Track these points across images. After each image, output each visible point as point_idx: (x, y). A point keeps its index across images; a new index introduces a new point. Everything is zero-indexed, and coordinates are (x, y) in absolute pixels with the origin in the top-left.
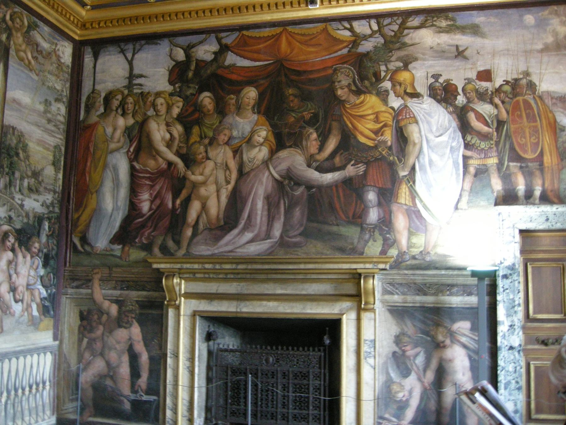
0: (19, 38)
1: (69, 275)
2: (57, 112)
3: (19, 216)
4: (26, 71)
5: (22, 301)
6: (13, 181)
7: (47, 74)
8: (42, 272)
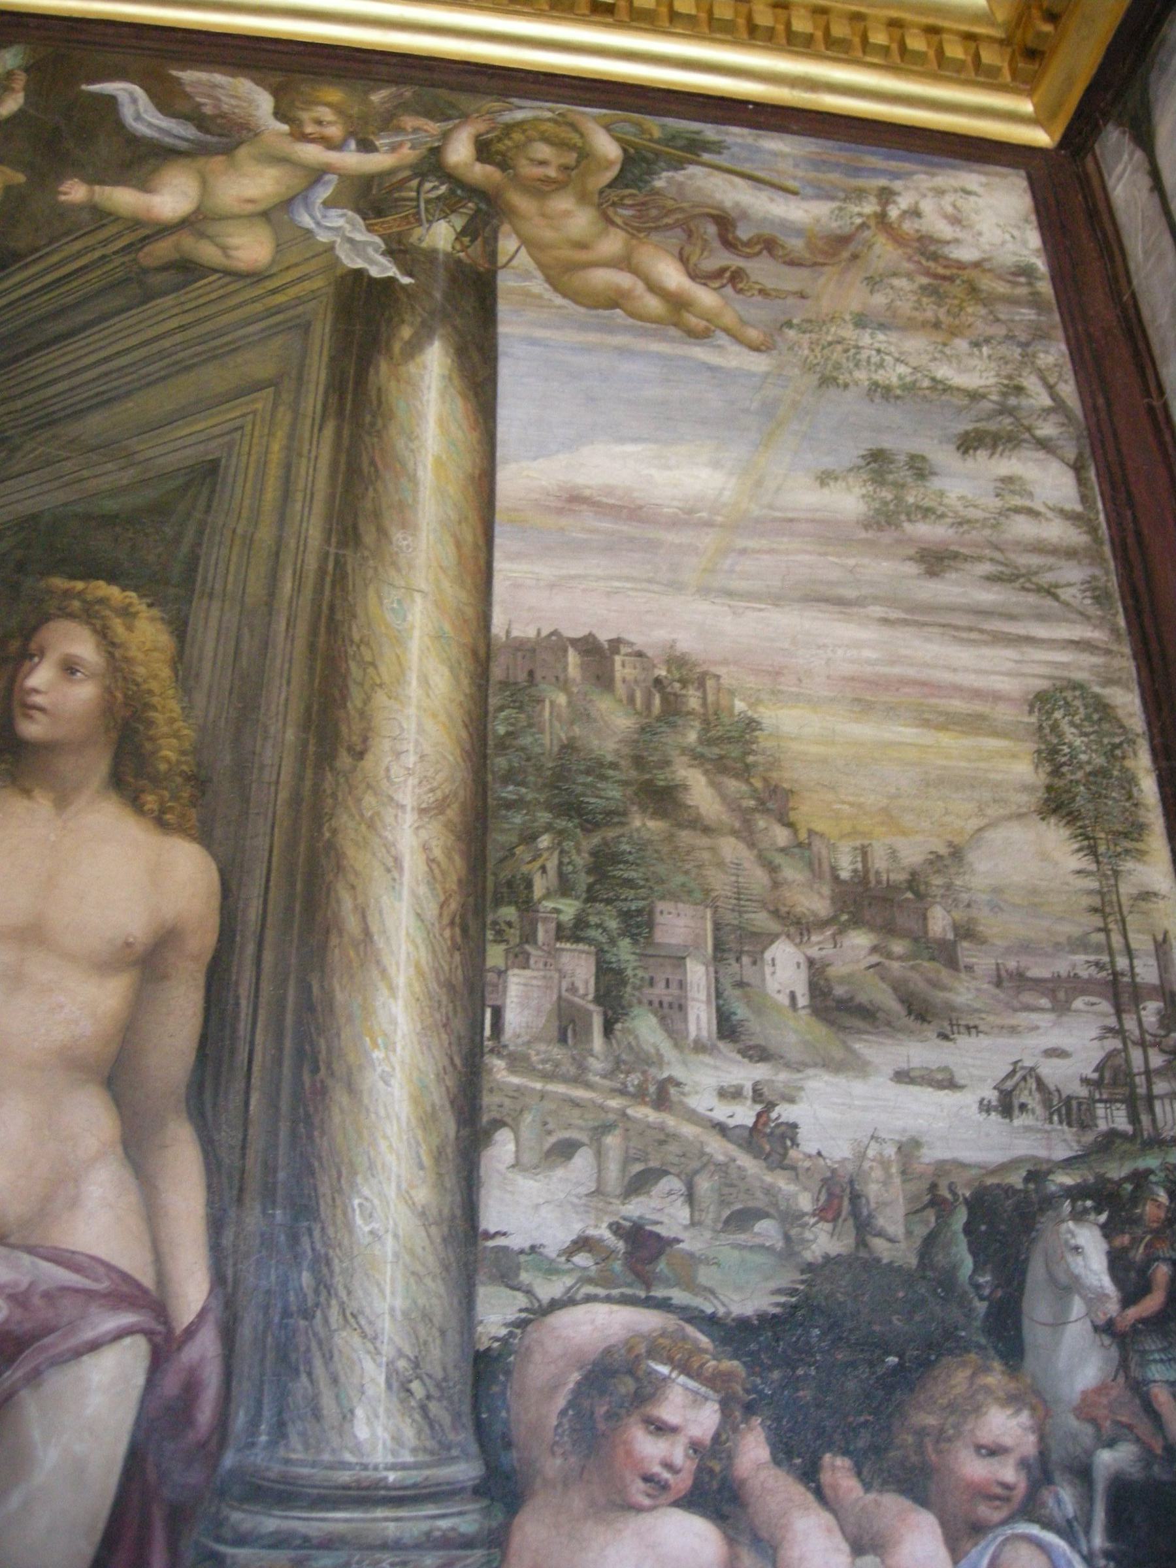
2: (996, 503)
3: (742, 1219)
7: (849, 332)
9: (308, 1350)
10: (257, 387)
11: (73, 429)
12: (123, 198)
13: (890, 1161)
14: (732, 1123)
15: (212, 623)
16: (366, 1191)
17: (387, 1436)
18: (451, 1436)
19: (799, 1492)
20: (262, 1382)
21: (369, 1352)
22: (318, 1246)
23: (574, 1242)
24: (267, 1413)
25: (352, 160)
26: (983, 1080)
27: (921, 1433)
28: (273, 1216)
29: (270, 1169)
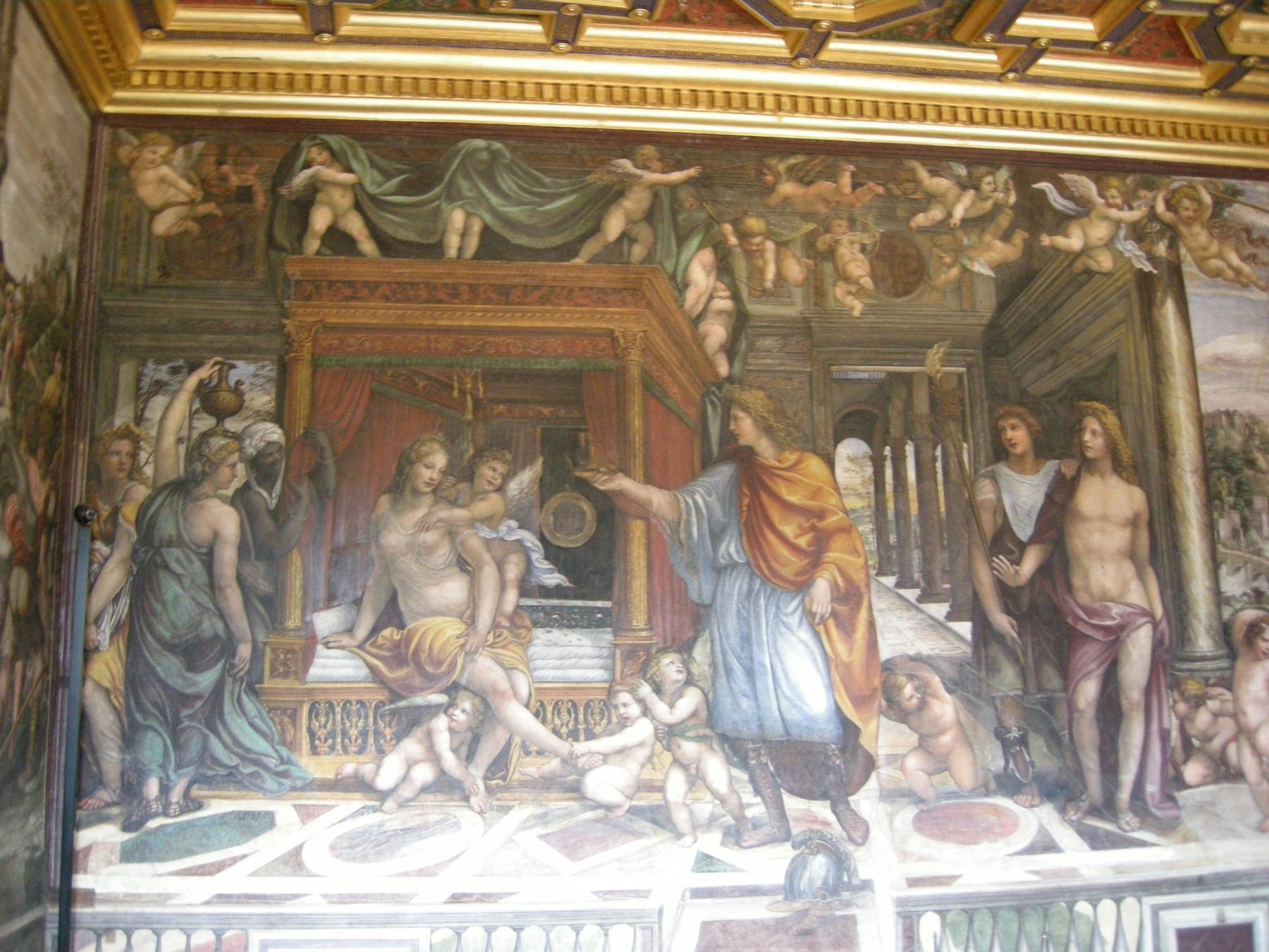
0: (1198, 235)
4: (1234, 293)
6: (1249, 518)
10: (1119, 324)
11: (1072, 344)
12: (1060, 241)
15: (1128, 413)
25: (1128, 215)
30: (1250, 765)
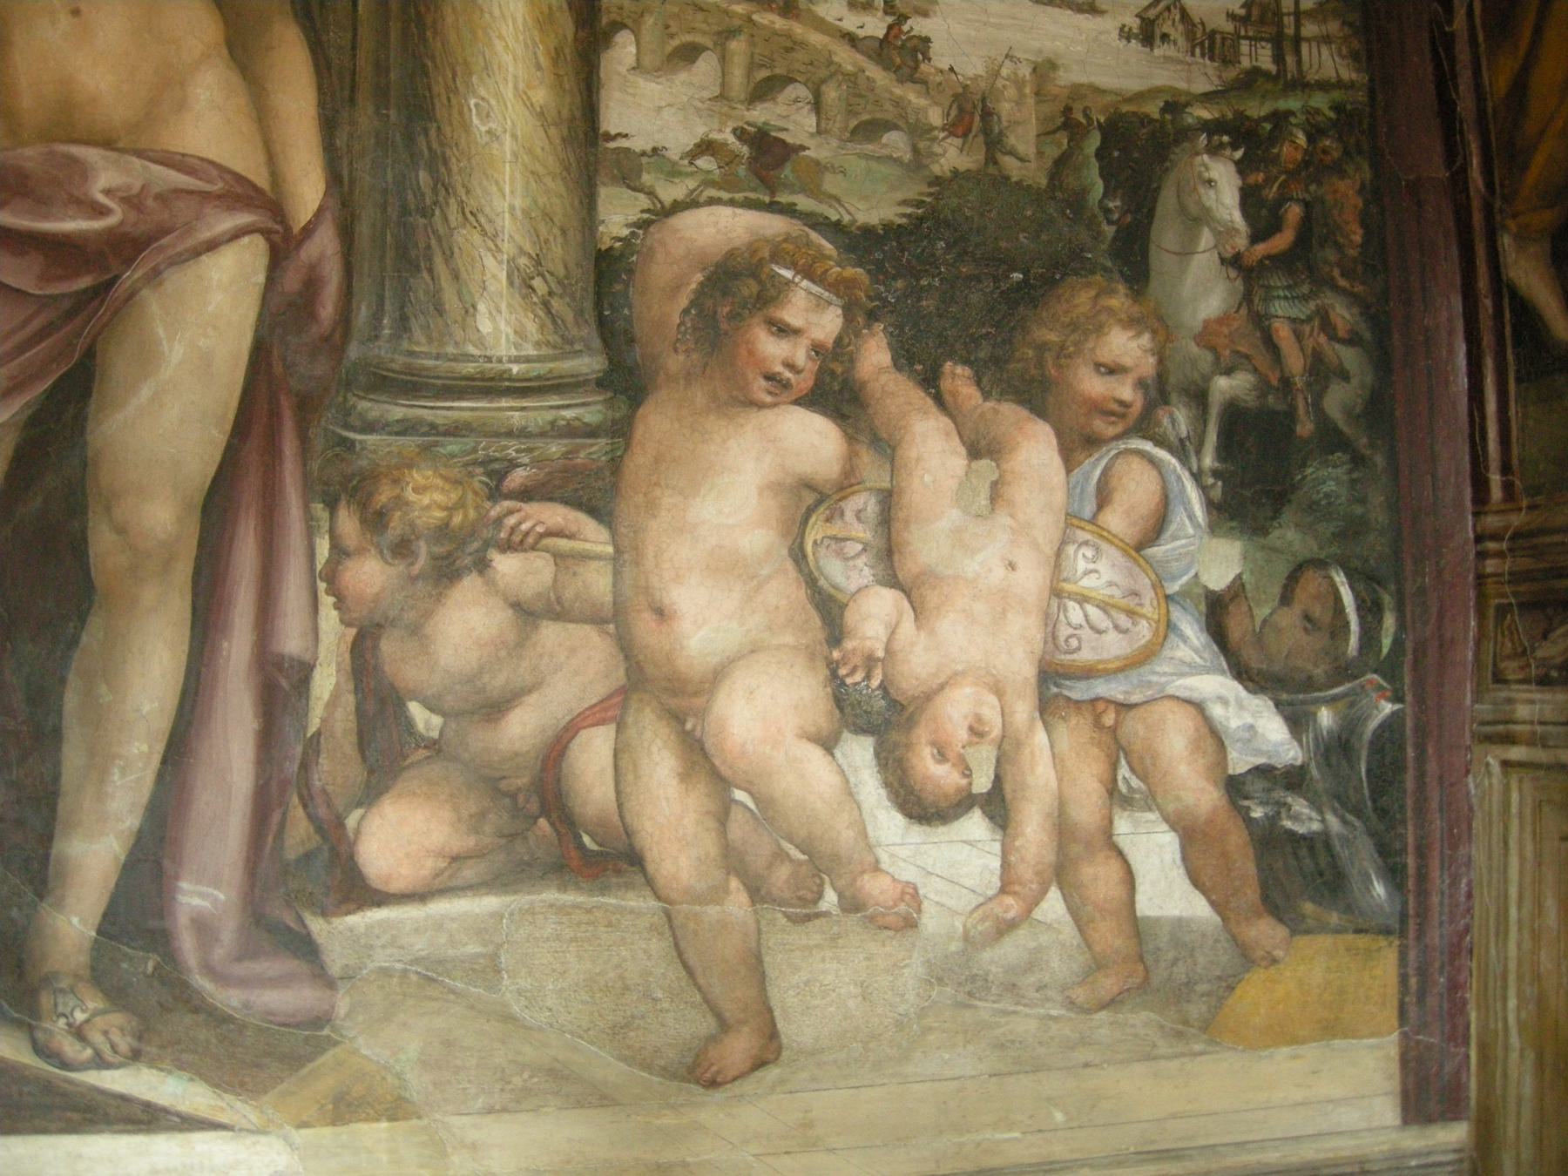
1: (1516, 578)
3: (870, 130)
5: (997, 805)
8: (1221, 563)
9: (429, 247)
13: (1024, 81)
14: (861, 33)
16: (482, 92)
17: (510, 331)
18: (574, 332)
19: (919, 397)
20: (383, 279)
21: (489, 249)
22: (435, 145)
23: (698, 146)
24: (388, 307)
26: (1125, 6)
27: (1042, 348)
28: (388, 116)
29: (381, 68)
30: (670, 818)
